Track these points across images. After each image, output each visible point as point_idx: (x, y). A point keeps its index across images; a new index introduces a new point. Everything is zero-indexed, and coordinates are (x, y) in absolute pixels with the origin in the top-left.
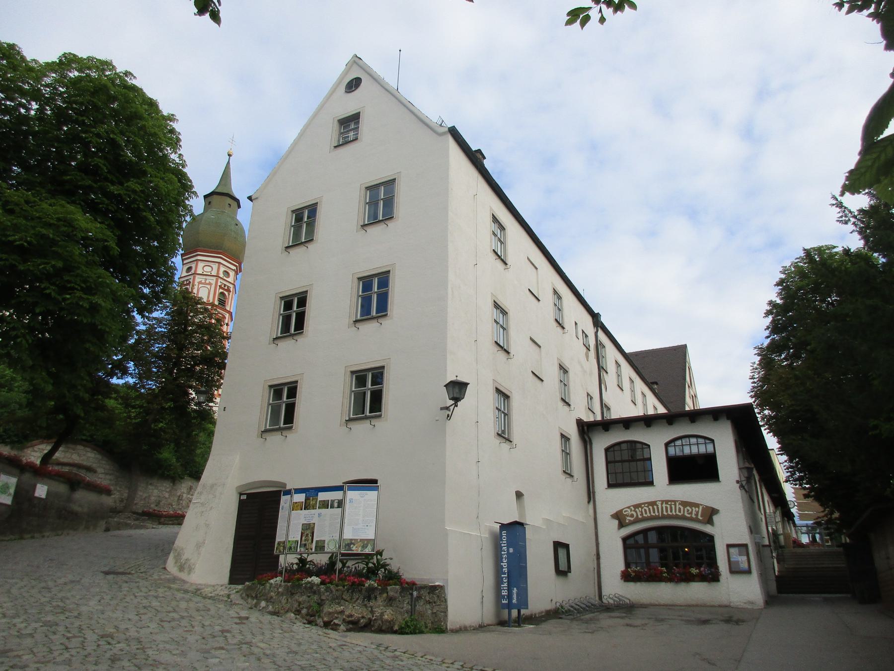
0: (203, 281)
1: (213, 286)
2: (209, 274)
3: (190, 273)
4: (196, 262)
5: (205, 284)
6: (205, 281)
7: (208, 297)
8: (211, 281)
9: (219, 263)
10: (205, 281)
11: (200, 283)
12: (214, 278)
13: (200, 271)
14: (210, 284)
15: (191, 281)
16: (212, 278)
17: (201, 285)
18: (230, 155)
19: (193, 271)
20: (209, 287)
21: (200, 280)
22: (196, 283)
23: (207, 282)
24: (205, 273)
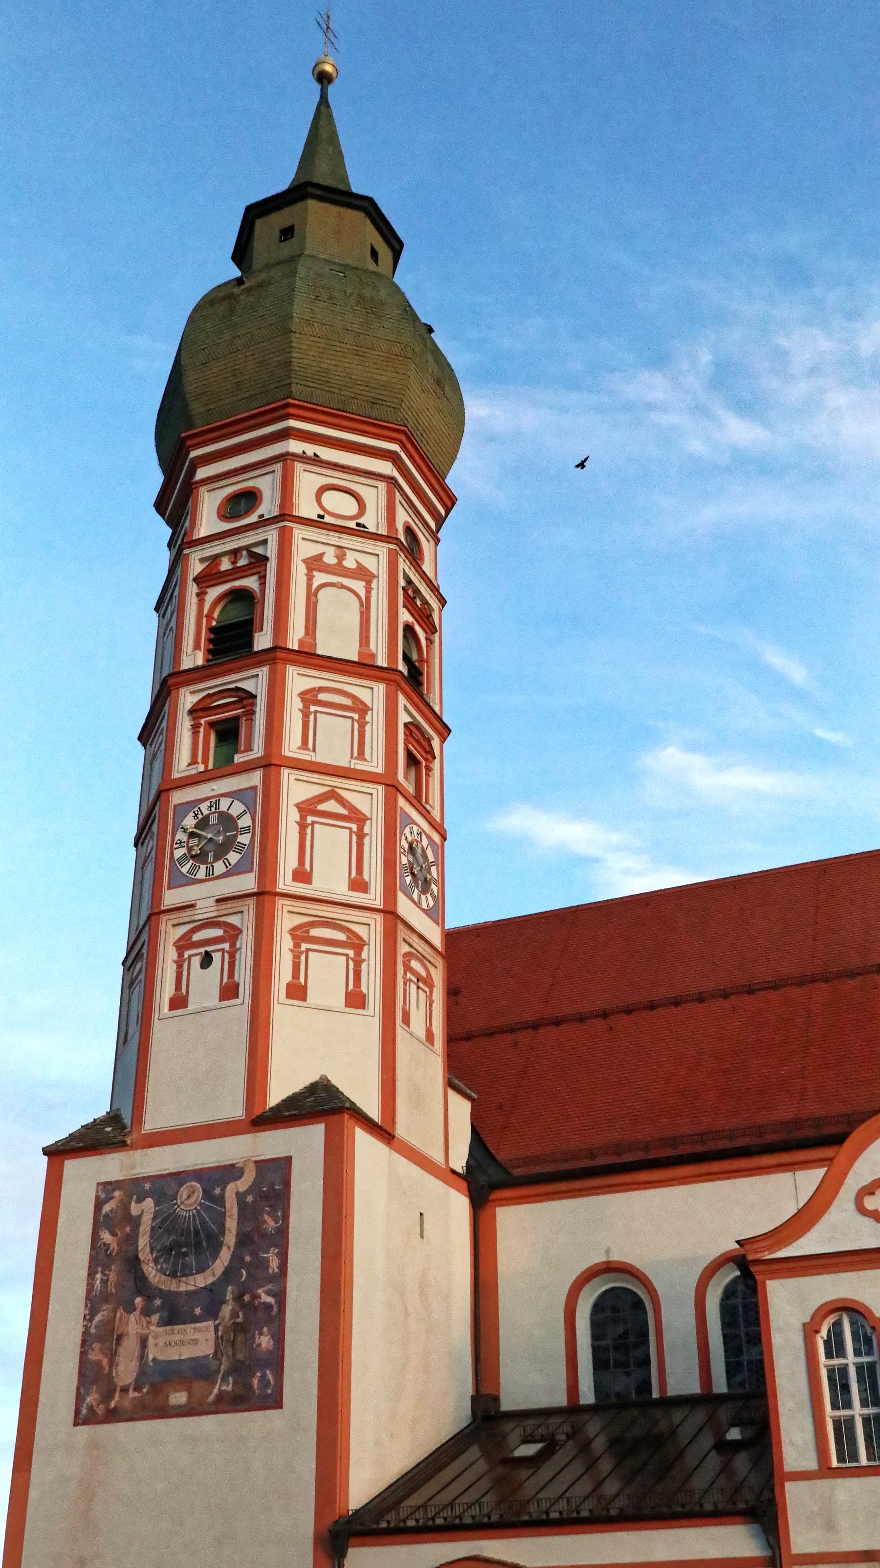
0: (330, 558)
1: (380, 587)
2: (352, 524)
3: (253, 518)
4: (278, 467)
5: (339, 569)
6: (341, 557)
7: (364, 638)
8: (370, 563)
9: (390, 481)
10: (341, 557)
11: (315, 564)
12: (382, 549)
13: (306, 507)
14: (363, 574)
15: (271, 551)
16: (369, 545)
17: (320, 578)
18: (323, 79)
19: (267, 507)
20: (359, 586)
21: (313, 550)
22: (299, 572)
23: (350, 563)
24: (328, 519)
